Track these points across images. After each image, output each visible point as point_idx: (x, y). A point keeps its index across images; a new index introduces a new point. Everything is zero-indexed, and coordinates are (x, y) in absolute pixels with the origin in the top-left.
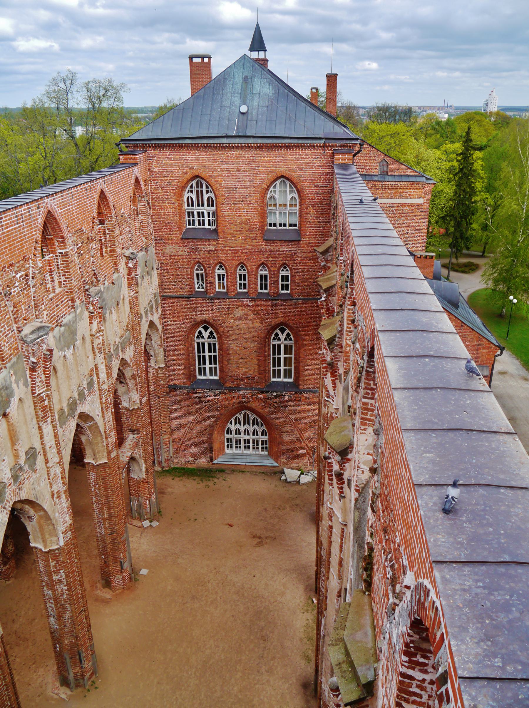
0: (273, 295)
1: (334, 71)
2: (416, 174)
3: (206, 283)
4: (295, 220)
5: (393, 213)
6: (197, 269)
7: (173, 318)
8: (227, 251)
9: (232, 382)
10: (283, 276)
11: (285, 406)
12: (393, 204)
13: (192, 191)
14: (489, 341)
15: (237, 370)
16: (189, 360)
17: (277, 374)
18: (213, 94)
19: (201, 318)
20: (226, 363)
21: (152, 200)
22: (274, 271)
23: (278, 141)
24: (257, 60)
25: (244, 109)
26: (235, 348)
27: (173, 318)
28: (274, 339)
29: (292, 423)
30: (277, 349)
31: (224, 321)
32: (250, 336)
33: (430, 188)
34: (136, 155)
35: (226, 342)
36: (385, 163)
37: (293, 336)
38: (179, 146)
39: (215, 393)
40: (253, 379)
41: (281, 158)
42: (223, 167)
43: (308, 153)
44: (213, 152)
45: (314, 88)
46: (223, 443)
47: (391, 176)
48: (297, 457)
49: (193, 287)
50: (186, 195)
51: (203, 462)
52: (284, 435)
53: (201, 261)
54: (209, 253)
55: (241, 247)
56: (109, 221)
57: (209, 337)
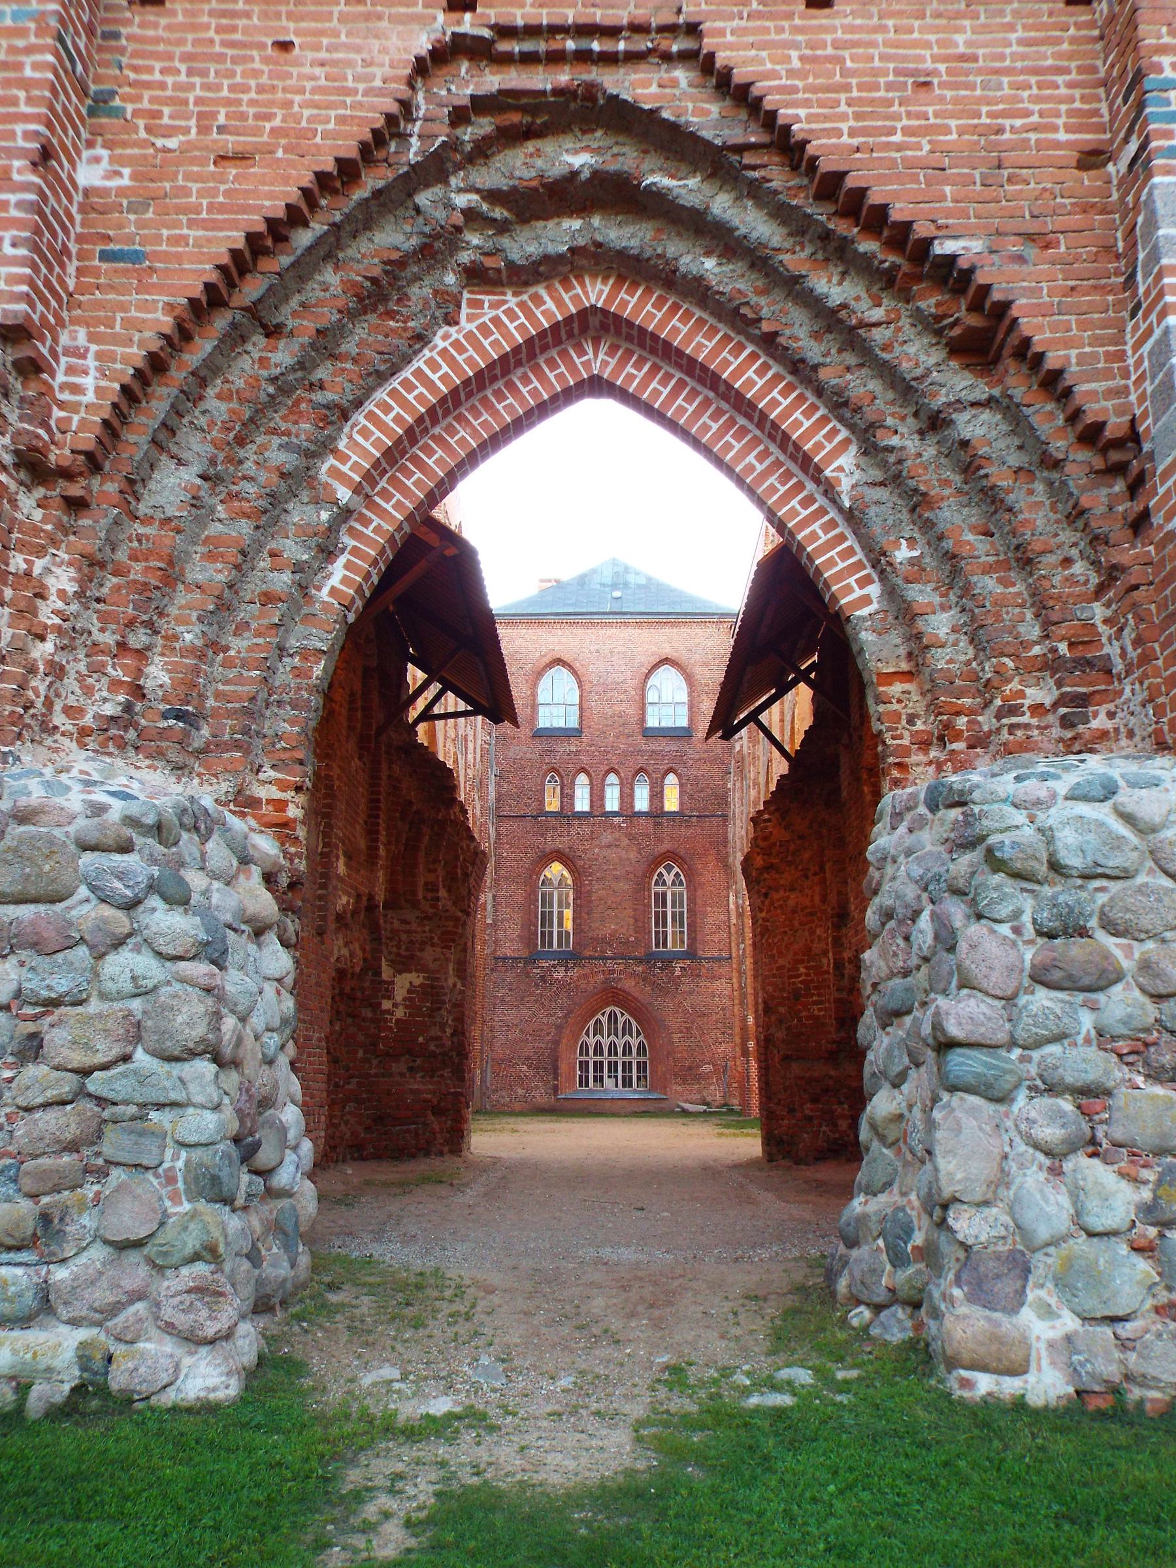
11: (677, 985)
28: (657, 883)
40: (627, 942)
48: (699, 1078)
51: (541, 1095)
52: (676, 1037)
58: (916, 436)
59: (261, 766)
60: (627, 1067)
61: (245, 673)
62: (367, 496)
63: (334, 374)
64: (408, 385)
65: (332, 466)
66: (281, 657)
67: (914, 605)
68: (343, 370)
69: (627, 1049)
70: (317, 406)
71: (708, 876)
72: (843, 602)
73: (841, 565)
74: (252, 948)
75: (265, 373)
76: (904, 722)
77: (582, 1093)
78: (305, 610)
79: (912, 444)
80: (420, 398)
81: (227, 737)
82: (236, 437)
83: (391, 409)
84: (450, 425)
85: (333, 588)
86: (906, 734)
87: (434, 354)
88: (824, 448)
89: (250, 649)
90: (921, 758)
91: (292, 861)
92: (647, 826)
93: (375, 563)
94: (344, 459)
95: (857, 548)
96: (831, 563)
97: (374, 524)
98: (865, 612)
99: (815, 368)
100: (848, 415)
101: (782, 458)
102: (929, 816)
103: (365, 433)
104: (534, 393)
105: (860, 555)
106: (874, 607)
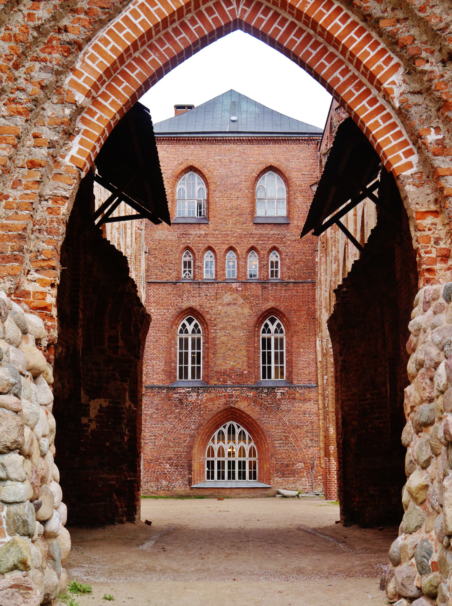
0: (263, 279)
3: (194, 268)
4: (283, 212)
6: (185, 256)
7: (157, 306)
8: (217, 235)
9: (218, 379)
10: (272, 262)
11: (278, 405)
13: (184, 184)
15: (223, 364)
16: (170, 354)
17: (267, 373)
19: (187, 305)
20: (212, 356)
22: (263, 254)
26: (222, 338)
27: (157, 306)
28: (264, 332)
29: (286, 427)
30: (266, 343)
31: (211, 308)
32: (239, 324)
35: (212, 331)
37: (284, 327)
38: (177, 140)
39: (198, 392)
40: (242, 375)
41: (270, 151)
42: (216, 158)
43: (294, 147)
44: (207, 147)
46: (204, 468)
48: (293, 473)
49: (179, 272)
52: (277, 443)
53: (190, 245)
54: (199, 237)
55: (231, 231)
57: (193, 332)
58: (440, 64)
59: (29, 271)
60: (242, 465)
61: (20, 213)
62: (93, 98)
63: (73, 22)
64: (119, 27)
65: (72, 79)
66: (40, 201)
67: (439, 170)
68: (79, 19)
69: (242, 452)
70: (63, 43)
71: (301, 326)
72: (394, 166)
73: (394, 143)
74: (33, 385)
75: (31, 24)
76: (432, 243)
77: (210, 484)
78: (55, 171)
79: (438, 69)
80: (127, 36)
81: (9, 253)
82: (14, 64)
83: (109, 43)
84: (145, 51)
85: (72, 156)
86: (434, 250)
87: (136, 7)
88: (383, 69)
89: (21, 197)
90: (443, 265)
91: (49, 330)
92: (256, 290)
93: (99, 140)
94: (79, 75)
95: (404, 132)
96: (387, 141)
97: (98, 115)
98: (408, 173)
99: (377, 21)
100: (398, 49)
101: (357, 73)
102: (446, 304)
103: (93, 58)
104: (199, 30)
105: (405, 136)
106: (414, 170)
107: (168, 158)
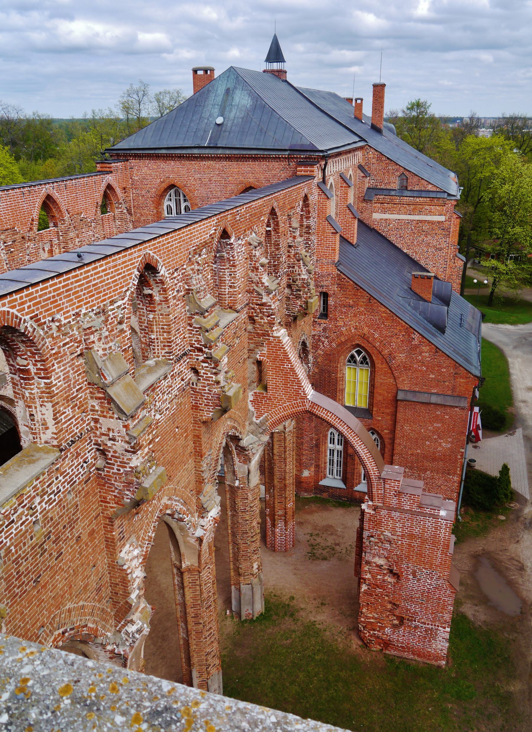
1: (383, 81)
2: (438, 190)
5: (412, 230)
12: (412, 221)
14: (466, 370)
18: (196, 106)
21: (134, 207)
23: (244, 152)
24: (272, 72)
25: (220, 120)
33: (452, 205)
34: (111, 163)
36: (405, 178)
42: (196, 176)
43: (276, 164)
45: (359, 99)
47: (411, 190)
50: (166, 203)
56: (62, 224)
107: (151, 175)
